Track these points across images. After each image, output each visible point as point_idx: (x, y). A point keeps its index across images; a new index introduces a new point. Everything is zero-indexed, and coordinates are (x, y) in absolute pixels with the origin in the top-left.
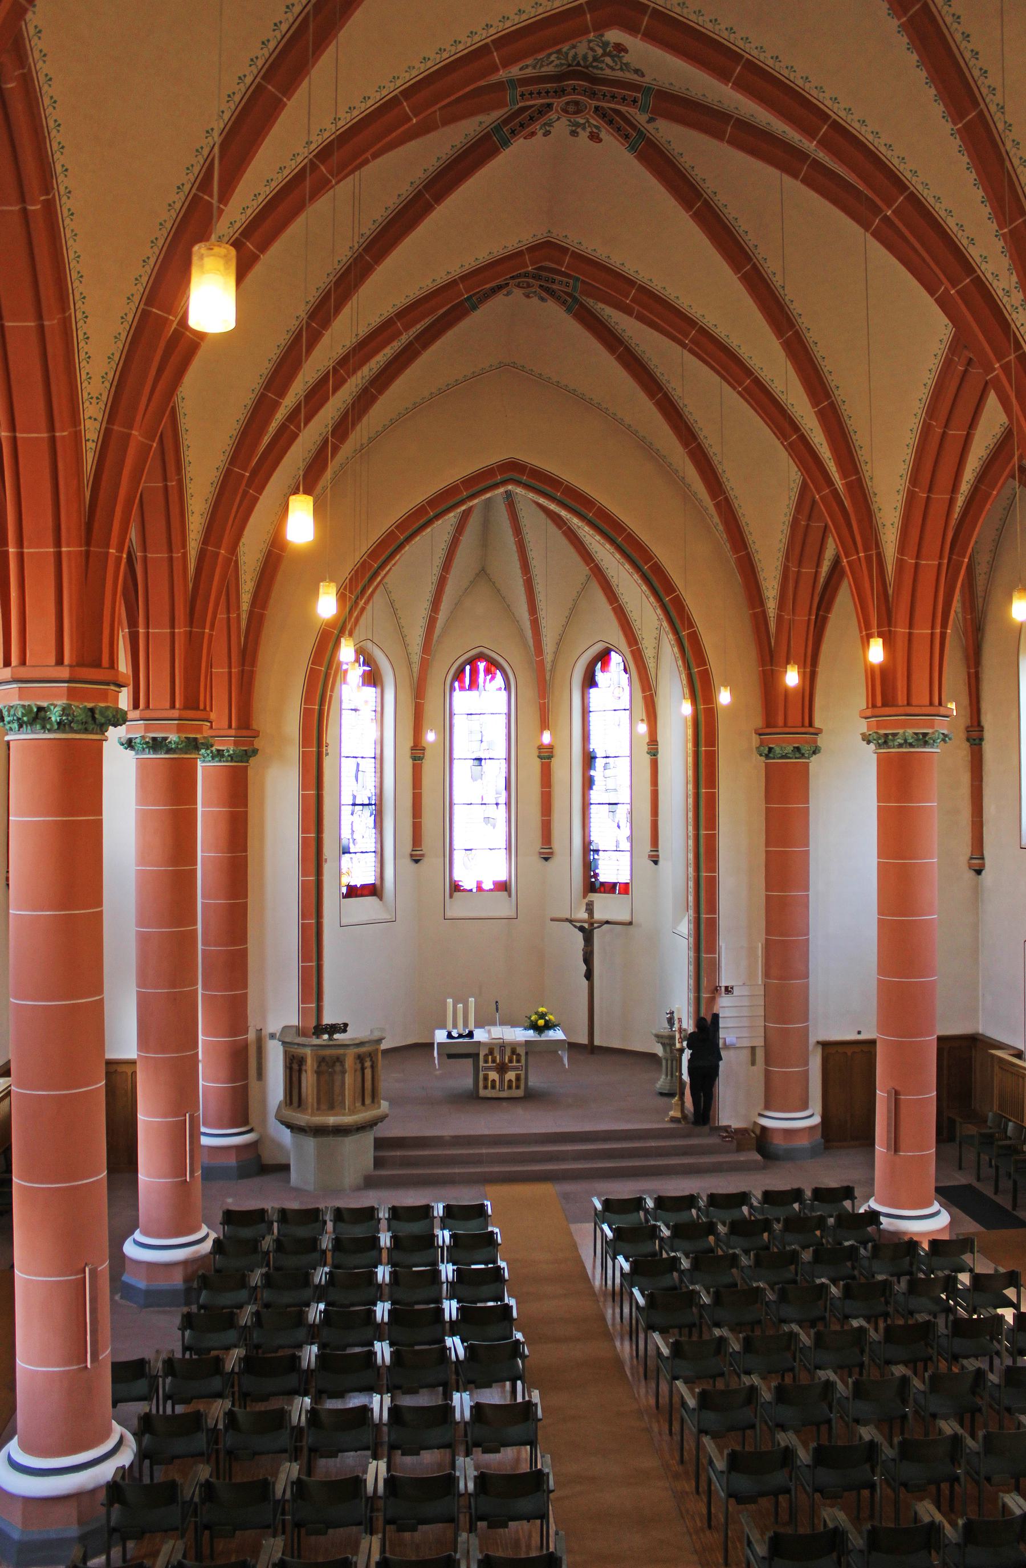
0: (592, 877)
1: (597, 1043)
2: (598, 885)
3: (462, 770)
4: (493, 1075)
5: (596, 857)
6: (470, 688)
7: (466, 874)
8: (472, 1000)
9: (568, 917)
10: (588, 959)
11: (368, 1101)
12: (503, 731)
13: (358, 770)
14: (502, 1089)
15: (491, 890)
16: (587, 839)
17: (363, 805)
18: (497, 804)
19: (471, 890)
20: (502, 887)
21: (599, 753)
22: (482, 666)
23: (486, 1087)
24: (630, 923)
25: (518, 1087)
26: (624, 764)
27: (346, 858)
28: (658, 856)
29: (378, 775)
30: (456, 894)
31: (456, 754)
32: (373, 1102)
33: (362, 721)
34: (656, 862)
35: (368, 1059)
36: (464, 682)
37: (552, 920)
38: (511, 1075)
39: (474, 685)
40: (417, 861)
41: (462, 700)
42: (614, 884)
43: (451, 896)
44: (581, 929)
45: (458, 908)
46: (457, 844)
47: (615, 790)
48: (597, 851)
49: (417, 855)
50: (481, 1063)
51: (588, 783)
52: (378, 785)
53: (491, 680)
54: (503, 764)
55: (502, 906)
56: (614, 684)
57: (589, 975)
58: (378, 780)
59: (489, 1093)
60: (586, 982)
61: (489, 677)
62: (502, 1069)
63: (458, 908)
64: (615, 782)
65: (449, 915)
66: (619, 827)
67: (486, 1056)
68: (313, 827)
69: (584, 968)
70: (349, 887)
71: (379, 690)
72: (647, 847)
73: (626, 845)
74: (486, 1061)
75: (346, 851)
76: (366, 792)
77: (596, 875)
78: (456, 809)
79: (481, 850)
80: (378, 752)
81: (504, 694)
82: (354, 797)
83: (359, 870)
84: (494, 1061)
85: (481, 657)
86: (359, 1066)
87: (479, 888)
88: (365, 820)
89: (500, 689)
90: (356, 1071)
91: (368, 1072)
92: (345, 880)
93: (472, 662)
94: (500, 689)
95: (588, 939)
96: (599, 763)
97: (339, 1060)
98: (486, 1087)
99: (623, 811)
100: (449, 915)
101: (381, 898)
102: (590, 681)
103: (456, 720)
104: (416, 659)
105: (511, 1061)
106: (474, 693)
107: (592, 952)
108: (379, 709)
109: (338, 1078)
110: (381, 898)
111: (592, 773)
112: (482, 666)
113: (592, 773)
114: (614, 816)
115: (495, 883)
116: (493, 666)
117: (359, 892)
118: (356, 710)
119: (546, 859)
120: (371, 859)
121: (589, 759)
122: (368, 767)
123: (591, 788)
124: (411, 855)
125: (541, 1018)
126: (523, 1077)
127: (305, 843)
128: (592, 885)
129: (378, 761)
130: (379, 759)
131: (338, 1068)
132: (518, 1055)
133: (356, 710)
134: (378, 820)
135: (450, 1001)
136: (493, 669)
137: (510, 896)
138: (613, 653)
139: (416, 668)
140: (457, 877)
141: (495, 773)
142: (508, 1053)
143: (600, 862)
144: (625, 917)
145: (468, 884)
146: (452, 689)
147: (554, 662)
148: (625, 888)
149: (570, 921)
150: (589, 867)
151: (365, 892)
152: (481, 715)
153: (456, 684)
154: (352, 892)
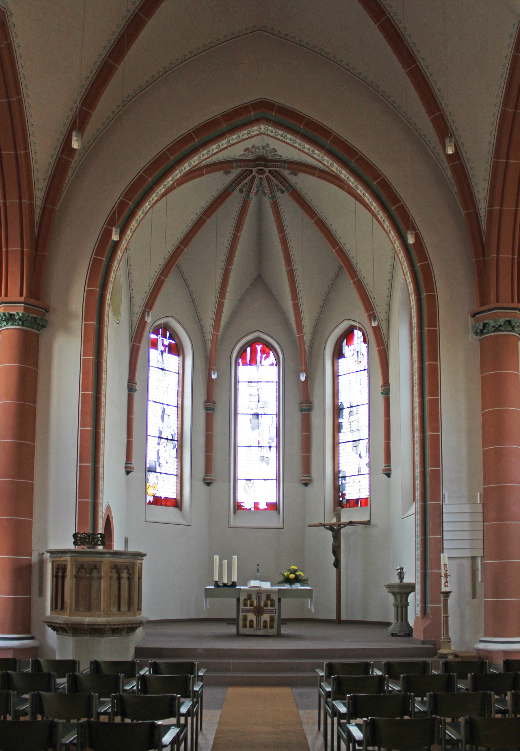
0: (340, 497)
1: (343, 618)
2: (344, 502)
3: (243, 423)
4: (251, 617)
5: (343, 481)
6: (250, 364)
9: (322, 522)
10: (336, 551)
11: (124, 608)
12: (275, 394)
13: (163, 413)
15: (265, 509)
16: (336, 469)
17: (167, 439)
18: (270, 447)
19: (250, 509)
20: (273, 507)
22: (259, 348)
23: (245, 626)
24: (368, 523)
25: (272, 627)
26: (364, 410)
27: (151, 476)
28: (390, 470)
29: (180, 419)
30: (239, 512)
31: (240, 410)
32: (129, 609)
33: (166, 378)
34: (388, 475)
35: (125, 571)
36: (246, 359)
38: (266, 617)
39: (253, 361)
41: (244, 372)
42: (357, 500)
43: (235, 513)
46: (240, 475)
47: (358, 430)
48: (344, 477)
49: (208, 479)
50: (241, 606)
51: (337, 428)
52: (180, 426)
53: (265, 358)
54: (275, 418)
55: (273, 521)
56: (356, 358)
57: (337, 564)
58: (180, 423)
59: (247, 631)
60: (335, 569)
61: (264, 356)
62: (259, 611)
63: (237, 521)
64: (357, 424)
65: (232, 524)
66: (360, 457)
67: (245, 600)
68: (91, 385)
69: (333, 558)
70: (155, 497)
71: (181, 358)
72: (382, 465)
73: (365, 470)
74: (245, 605)
75: (153, 470)
76: (171, 429)
77: (343, 495)
78: (240, 450)
79: (257, 478)
80: (180, 402)
81: (275, 368)
82: (160, 433)
83: (165, 486)
84: (252, 605)
85: (258, 340)
86: (116, 575)
88: (169, 452)
89: (272, 364)
90: (111, 578)
91: (125, 583)
92: (151, 491)
93: (252, 344)
94: (272, 364)
95: (337, 537)
96: (346, 412)
97: (96, 567)
98: (245, 626)
99: (363, 446)
100: (232, 524)
103: (240, 386)
104: (209, 337)
105: (266, 605)
106: (254, 367)
107: (339, 546)
108: (181, 372)
109: (95, 583)
111: (341, 420)
112: (259, 348)
113: (341, 420)
114: (357, 450)
115: (268, 504)
116: (268, 348)
117: (163, 503)
118: (163, 369)
119: (306, 485)
120: (173, 481)
121: (338, 410)
122: (172, 413)
123: (339, 431)
124: (204, 480)
125: (291, 573)
126: (276, 618)
127: (84, 399)
128: (340, 502)
129: (180, 410)
130: (181, 408)
131: (95, 574)
132: (272, 600)
133: (163, 369)
134: (179, 451)
135: (217, 557)
136: (267, 350)
137: (279, 513)
139: (209, 344)
140: (240, 499)
141: (269, 426)
143: (346, 485)
144: (366, 519)
145: (248, 504)
146: (237, 364)
147: (311, 347)
148: (365, 502)
149: (324, 525)
150: (338, 489)
152: (258, 386)
153: (240, 361)
154: (157, 501)
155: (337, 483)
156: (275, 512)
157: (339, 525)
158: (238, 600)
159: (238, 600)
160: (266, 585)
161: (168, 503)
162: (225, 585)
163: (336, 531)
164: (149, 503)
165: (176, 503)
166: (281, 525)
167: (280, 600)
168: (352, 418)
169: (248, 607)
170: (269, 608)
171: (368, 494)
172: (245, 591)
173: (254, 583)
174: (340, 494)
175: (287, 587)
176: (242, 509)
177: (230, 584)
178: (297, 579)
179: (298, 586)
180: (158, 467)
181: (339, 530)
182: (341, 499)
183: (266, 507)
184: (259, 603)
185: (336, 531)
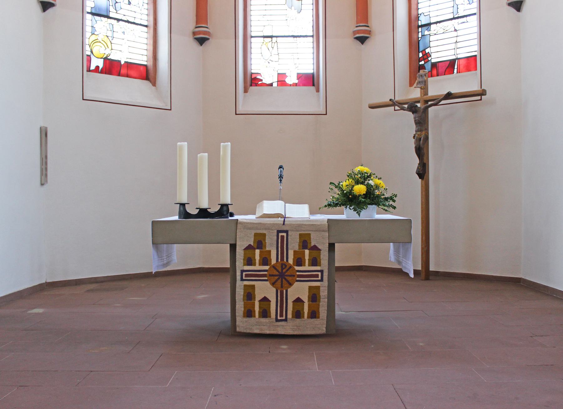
1: (432, 268)
4: (265, 289)
5: (426, 33)
7: (265, 63)
8: (226, 148)
14: (281, 318)
15: (296, 85)
16: (414, 13)
19: (271, 85)
20: (309, 80)
24: (483, 93)
25: (314, 314)
37: (372, 107)
38: (299, 290)
40: (201, 41)
43: (246, 91)
44: (412, 108)
45: (253, 102)
49: (200, 33)
57: (422, 172)
62: (282, 277)
65: (240, 109)
67: (249, 248)
69: (417, 161)
70: (106, 60)
77: (426, 56)
84: (265, 261)
87: (282, 82)
95: (422, 123)
98: (249, 313)
100: (240, 109)
101: (154, 84)
105: (299, 262)
110: (154, 84)
115: (299, 76)
117: (123, 71)
119: (362, 40)
124: (194, 33)
125: (357, 182)
126: (324, 293)
132: (315, 248)
137: (318, 91)
140: (255, 67)
142: (294, 244)
144: (475, 88)
151: (132, 73)
154: (111, 67)
155: (414, 36)
156: (313, 89)
157: (426, 102)
158: (233, 247)
159: (233, 247)
160: (299, 212)
161: (132, 73)
162: (203, 213)
163: (420, 111)
164: (97, 69)
165: (146, 74)
166: (322, 110)
167: (332, 247)
169: (257, 267)
170: (307, 267)
171: (476, 48)
172: (248, 226)
173: (271, 207)
174: (421, 55)
175: (347, 214)
176: (257, 85)
177: (214, 209)
178: (372, 198)
179: (373, 213)
180: (112, 9)
181: (426, 110)
182: (422, 63)
183: (297, 81)
184: (283, 258)
185: (420, 111)
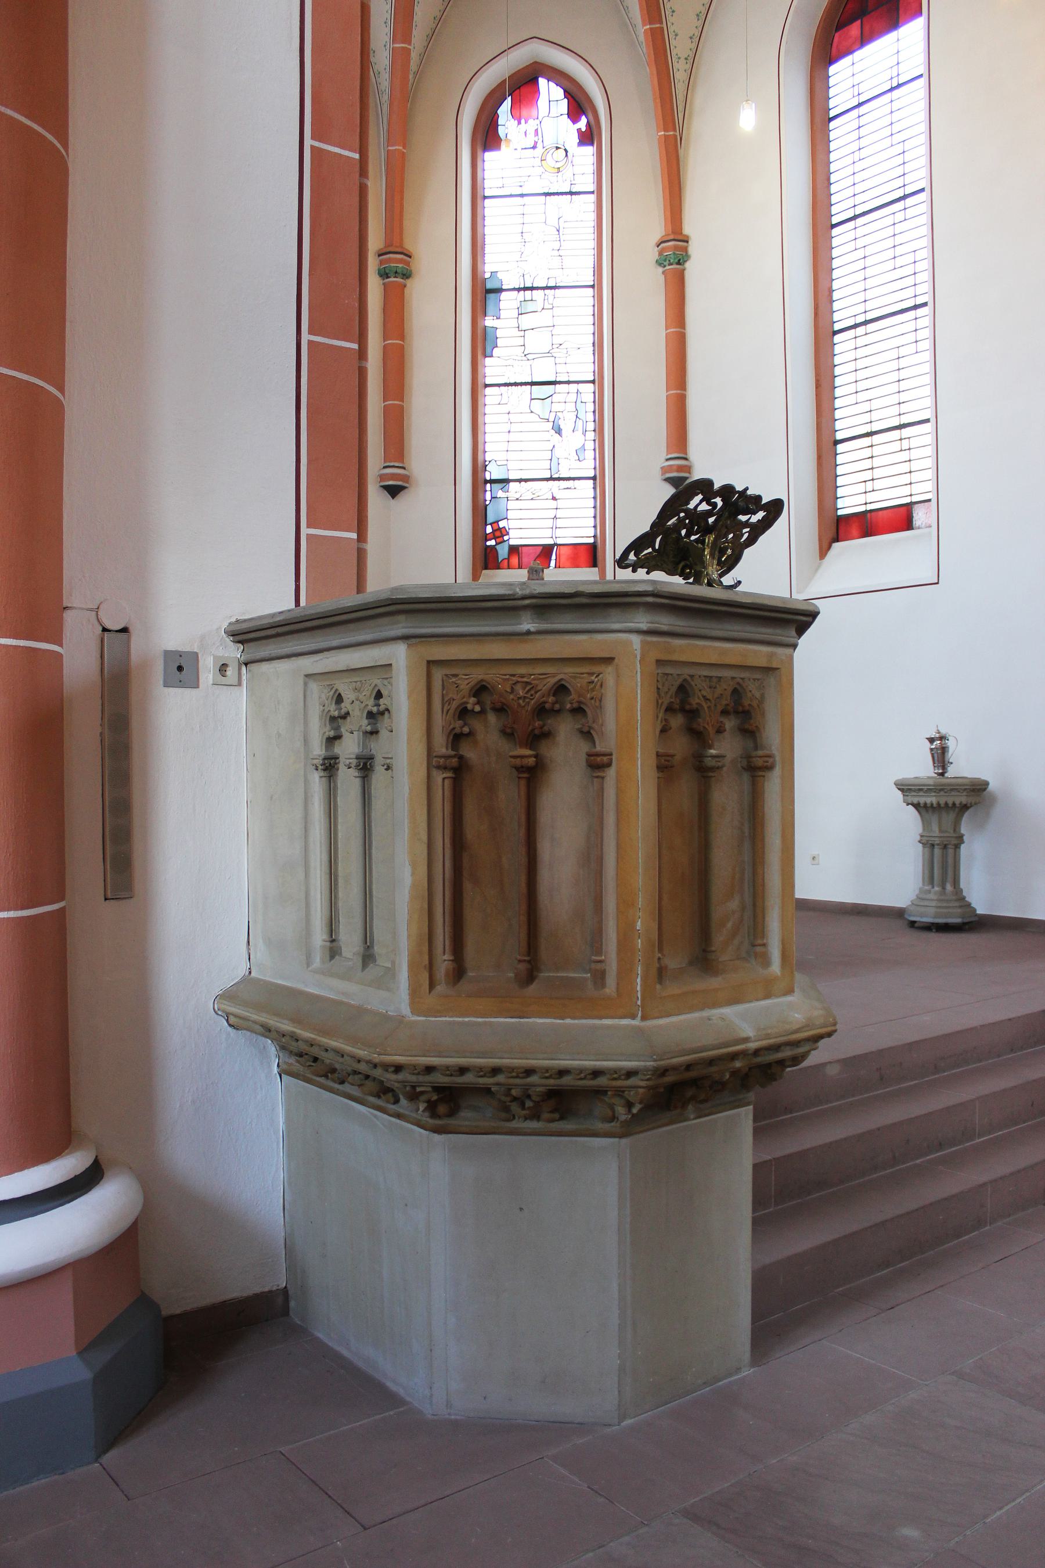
2: (503, 552)
5: (500, 494)
21: (509, 280)
51: (482, 343)
66: (559, 431)
77: (500, 533)
96: (508, 302)
102: (487, 136)
111: (489, 322)
113: (489, 322)
138: (542, 82)
168: (526, 321)
174: (489, 529)
182: (492, 543)
